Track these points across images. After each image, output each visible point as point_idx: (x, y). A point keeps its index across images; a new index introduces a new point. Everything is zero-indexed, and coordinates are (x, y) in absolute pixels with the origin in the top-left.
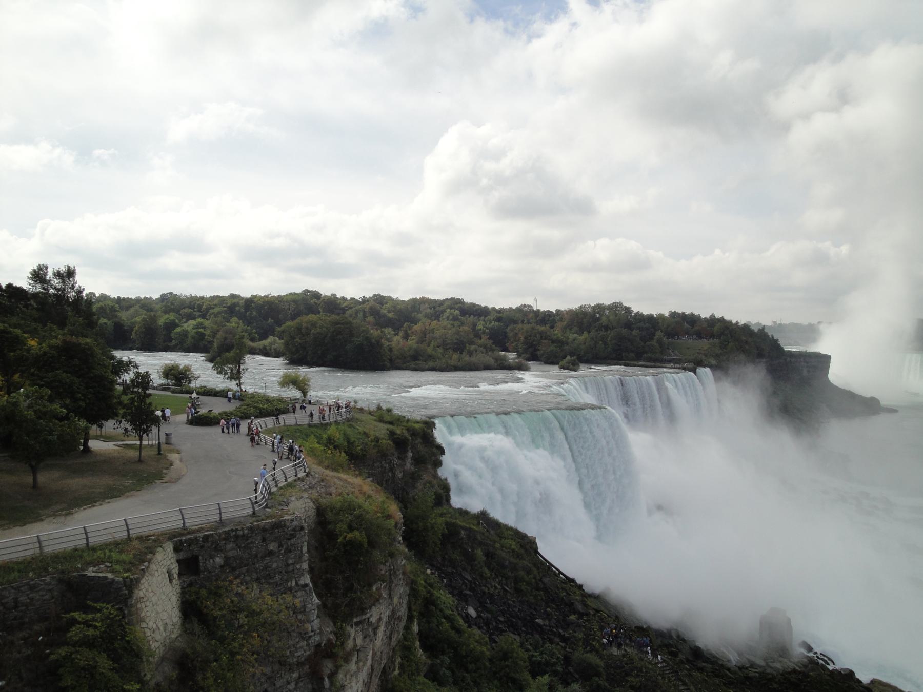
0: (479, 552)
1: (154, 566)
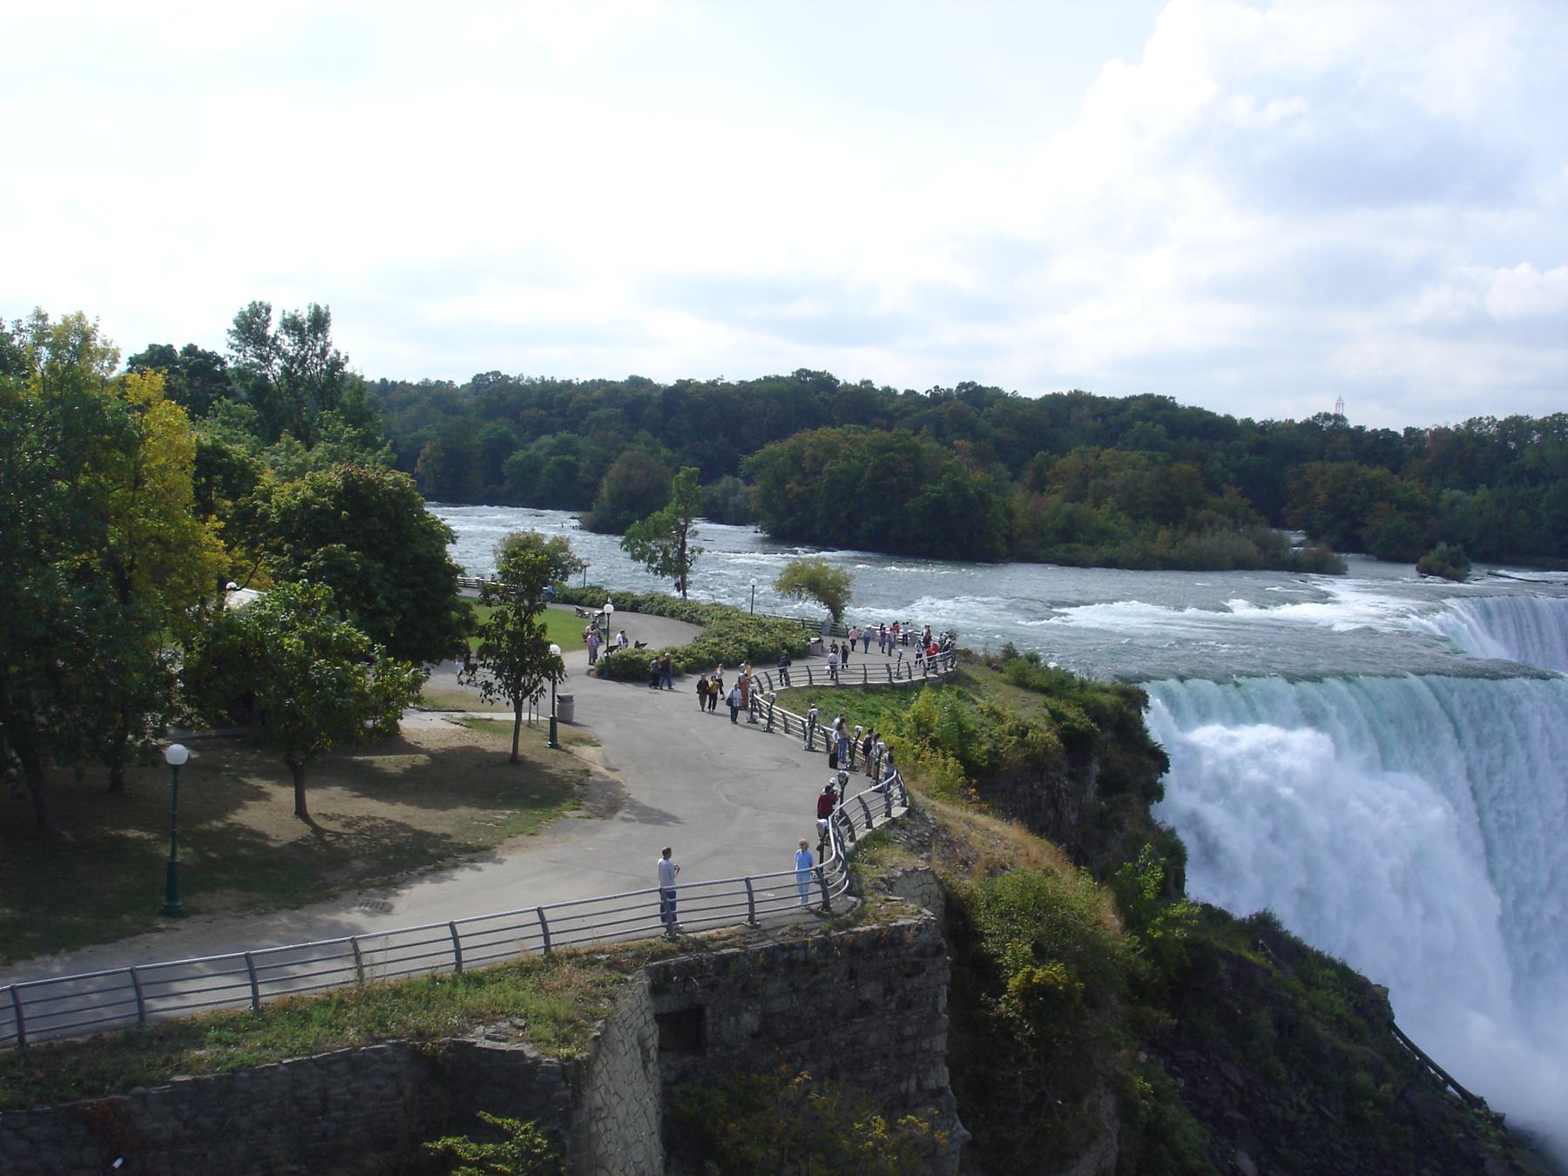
0: (1263, 1019)
1: (616, 1031)
